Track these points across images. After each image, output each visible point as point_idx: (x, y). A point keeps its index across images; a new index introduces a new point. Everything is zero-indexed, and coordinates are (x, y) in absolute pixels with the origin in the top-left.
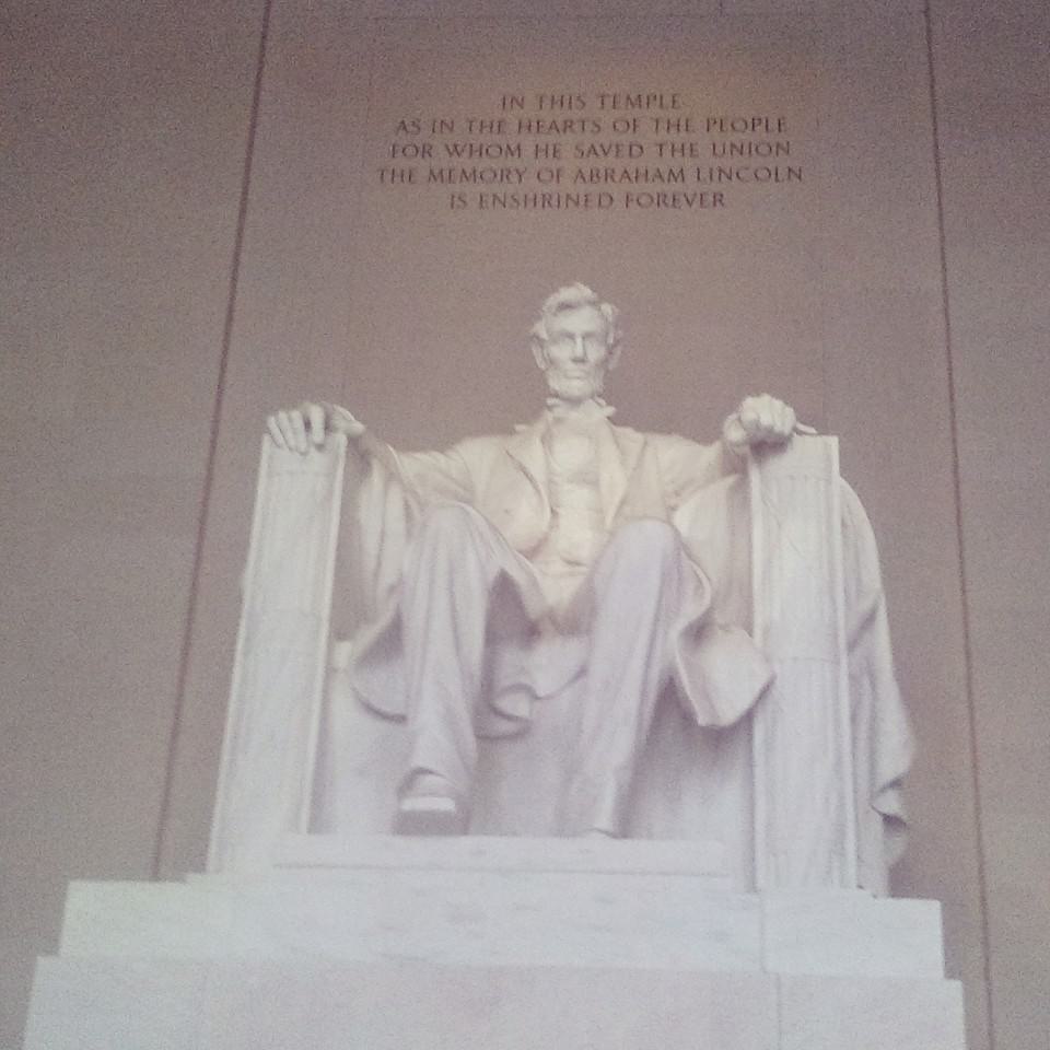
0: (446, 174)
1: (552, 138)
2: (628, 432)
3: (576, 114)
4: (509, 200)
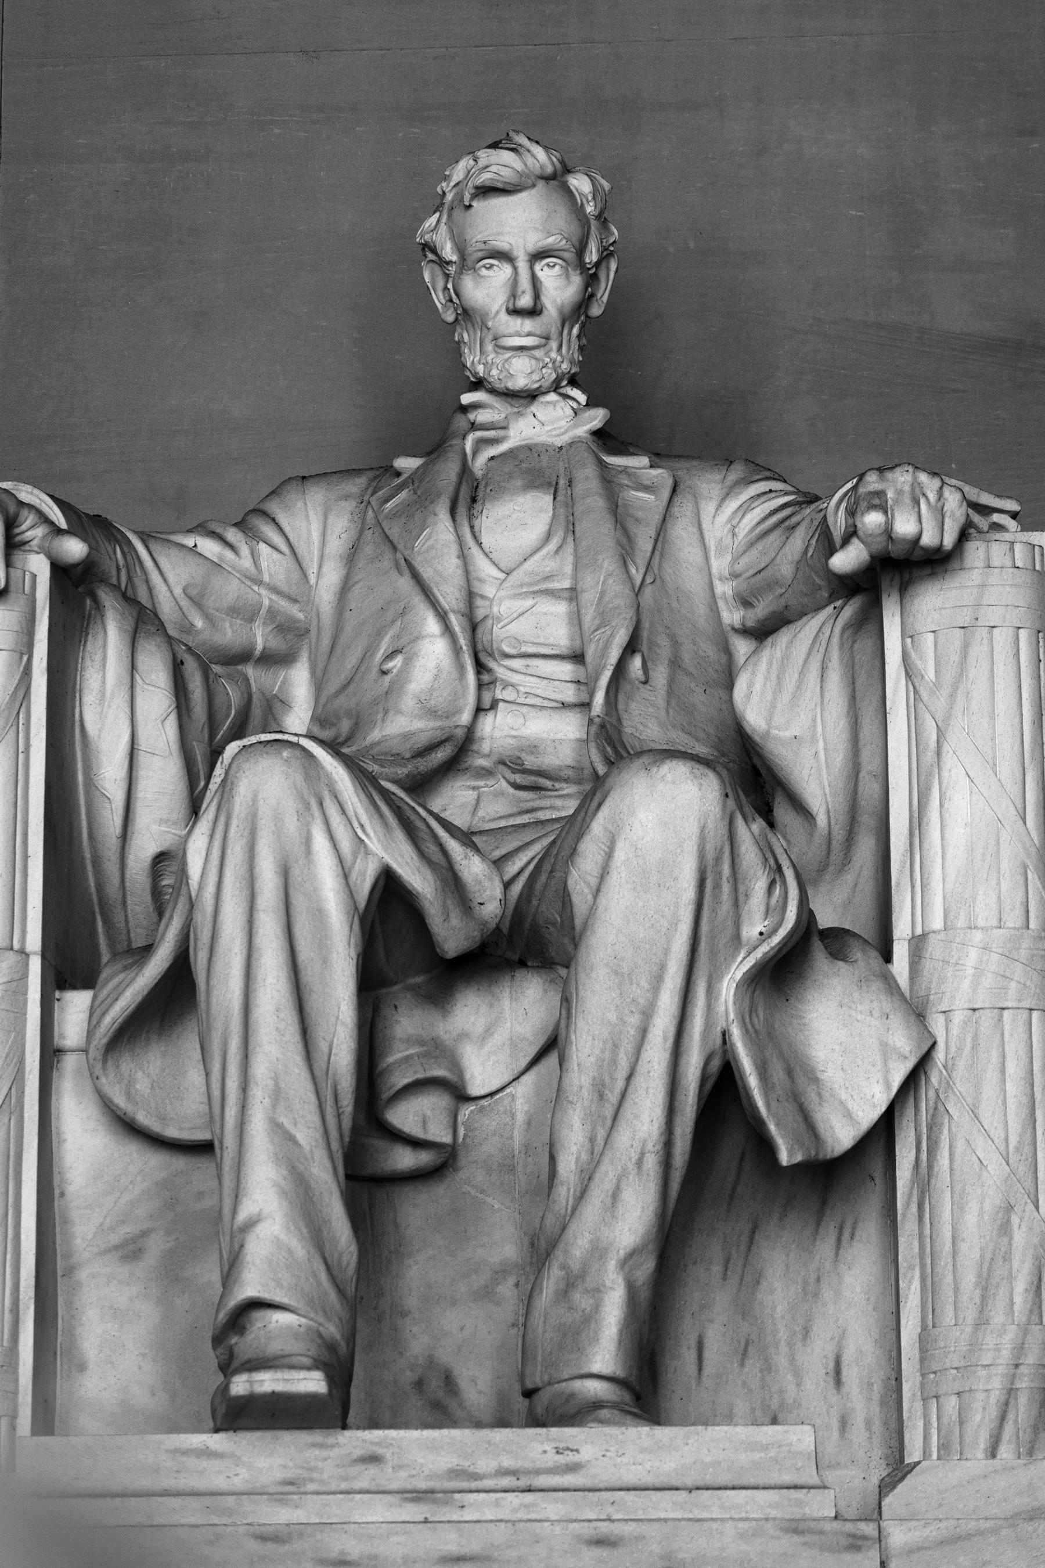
2: (639, 462)
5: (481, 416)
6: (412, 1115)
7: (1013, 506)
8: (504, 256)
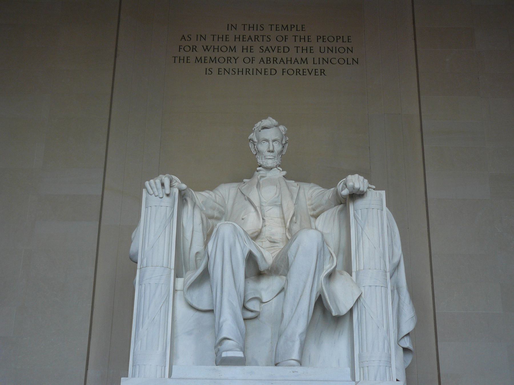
0: (203, 59)
1: (249, 43)
3: (259, 33)
4: (231, 71)
5: (261, 172)
6: (253, 305)
7: (374, 187)
8: (267, 141)
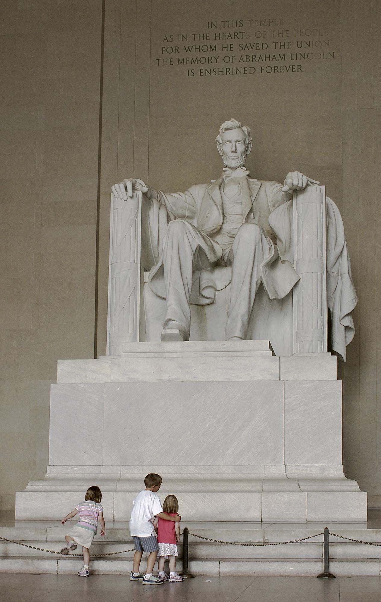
0: (185, 60)
4: (212, 72)
7: (318, 183)
8: (230, 142)
